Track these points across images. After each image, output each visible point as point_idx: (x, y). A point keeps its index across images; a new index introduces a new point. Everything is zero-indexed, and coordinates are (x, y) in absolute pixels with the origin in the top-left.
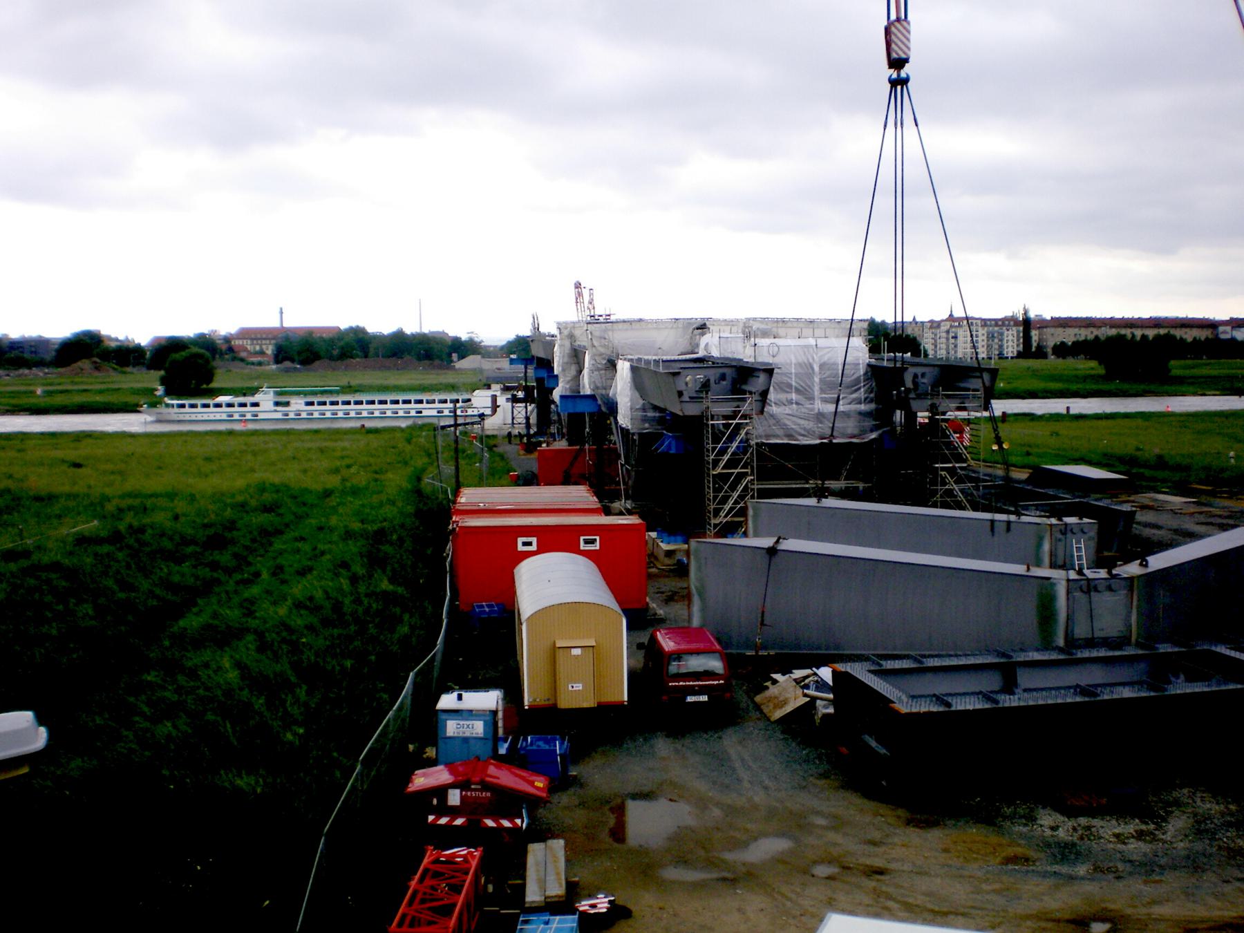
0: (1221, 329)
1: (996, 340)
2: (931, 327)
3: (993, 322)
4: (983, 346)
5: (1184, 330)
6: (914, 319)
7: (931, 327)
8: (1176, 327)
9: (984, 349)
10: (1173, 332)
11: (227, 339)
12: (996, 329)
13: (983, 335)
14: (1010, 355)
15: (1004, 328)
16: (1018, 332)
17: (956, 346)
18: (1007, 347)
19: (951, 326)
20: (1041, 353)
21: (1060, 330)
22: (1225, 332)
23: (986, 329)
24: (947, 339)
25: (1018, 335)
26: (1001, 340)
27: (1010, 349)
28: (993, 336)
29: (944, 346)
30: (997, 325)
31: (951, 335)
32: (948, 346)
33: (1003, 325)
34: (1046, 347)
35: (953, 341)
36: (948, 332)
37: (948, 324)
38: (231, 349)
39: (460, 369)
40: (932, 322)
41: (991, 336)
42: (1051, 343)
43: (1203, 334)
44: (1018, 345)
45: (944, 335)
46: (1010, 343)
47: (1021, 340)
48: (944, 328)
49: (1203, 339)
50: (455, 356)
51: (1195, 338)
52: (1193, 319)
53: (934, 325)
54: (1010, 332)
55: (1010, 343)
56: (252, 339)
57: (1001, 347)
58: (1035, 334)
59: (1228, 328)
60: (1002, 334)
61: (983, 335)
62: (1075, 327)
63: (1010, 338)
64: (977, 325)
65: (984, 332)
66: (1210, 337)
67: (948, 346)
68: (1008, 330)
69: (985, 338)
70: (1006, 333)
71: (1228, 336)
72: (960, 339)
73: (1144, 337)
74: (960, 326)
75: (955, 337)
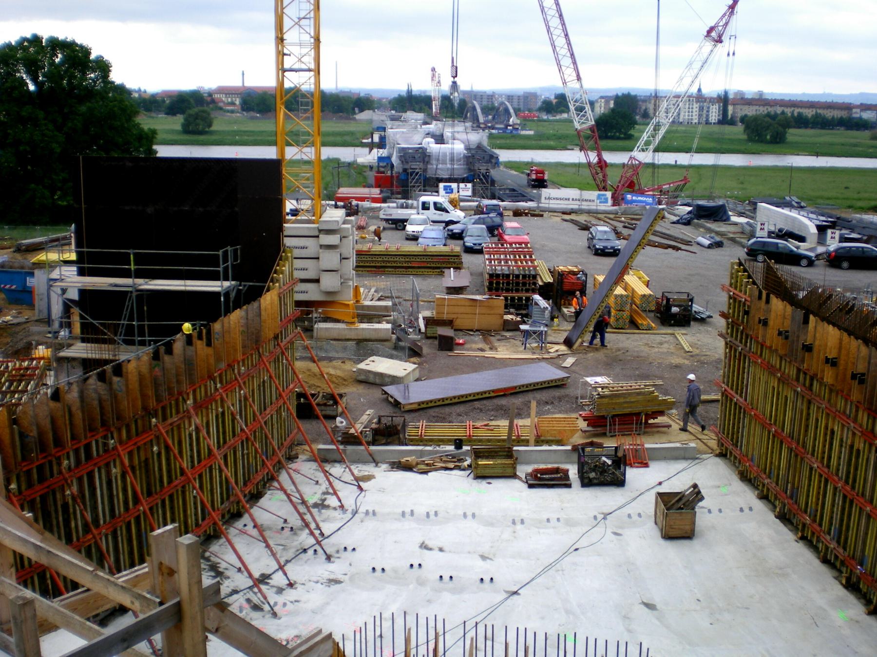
5: (829, 110)
10: (819, 111)
11: (210, 94)
14: (713, 121)
21: (747, 107)
22: (856, 113)
25: (719, 108)
26: (708, 111)
27: (714, 118)
28: (703, 108)
38: (213, 101)
39: (360, 120)
41: (701, 109)
43: (837, 114)
44: (719, 116)
46: (714, 114)
47: (721, 112)
49: (839, 116)
50: (357, 110)
52: (837, 103)
54: (714, 106)
55: (714, 114)
56: (226, 94)
57: (708, 116)
58: (730, 108)
59: (858, 110)
60: (709, 108)
62: (756, 105)
63: (714, 110)
65: (698, 105)
66: (844, 117)
69: (697, 109)
70: (711, 107)
71: (858, 116)
73: (783, 113)
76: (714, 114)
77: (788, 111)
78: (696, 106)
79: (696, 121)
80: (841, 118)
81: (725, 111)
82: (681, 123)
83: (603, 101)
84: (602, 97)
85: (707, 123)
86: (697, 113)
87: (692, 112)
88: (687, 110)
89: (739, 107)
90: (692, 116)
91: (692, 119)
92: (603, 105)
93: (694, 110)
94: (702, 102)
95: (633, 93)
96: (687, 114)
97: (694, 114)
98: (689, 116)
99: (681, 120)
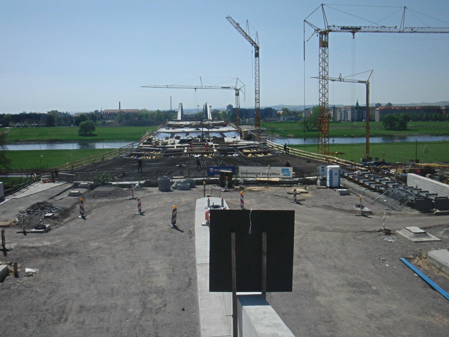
3: (360, 108)
4: (356, 116)
6: (334, 106)
9: (356, 117)
12: (360, 110)
13: (356, 112)
15: (363, 110)
18: (365, 116)
23: (357, 110)
30: (361, 109)
36: (344, 111)
45: (343, 112)
48: (343, 110)
53: (340, 109)
60: (363, 112)
61: (356, 112)
65: (357, 111)
68: (365, 111)
69: (357, 113)
70: (364, 112)
72: (349, 114)
75: (347, 113)
78: (356, 111)
83: (307, 111)
87: (354, 115)
90: (354, 117)
93: (355, 114)
94: (358, 109)
97: (355, 116)
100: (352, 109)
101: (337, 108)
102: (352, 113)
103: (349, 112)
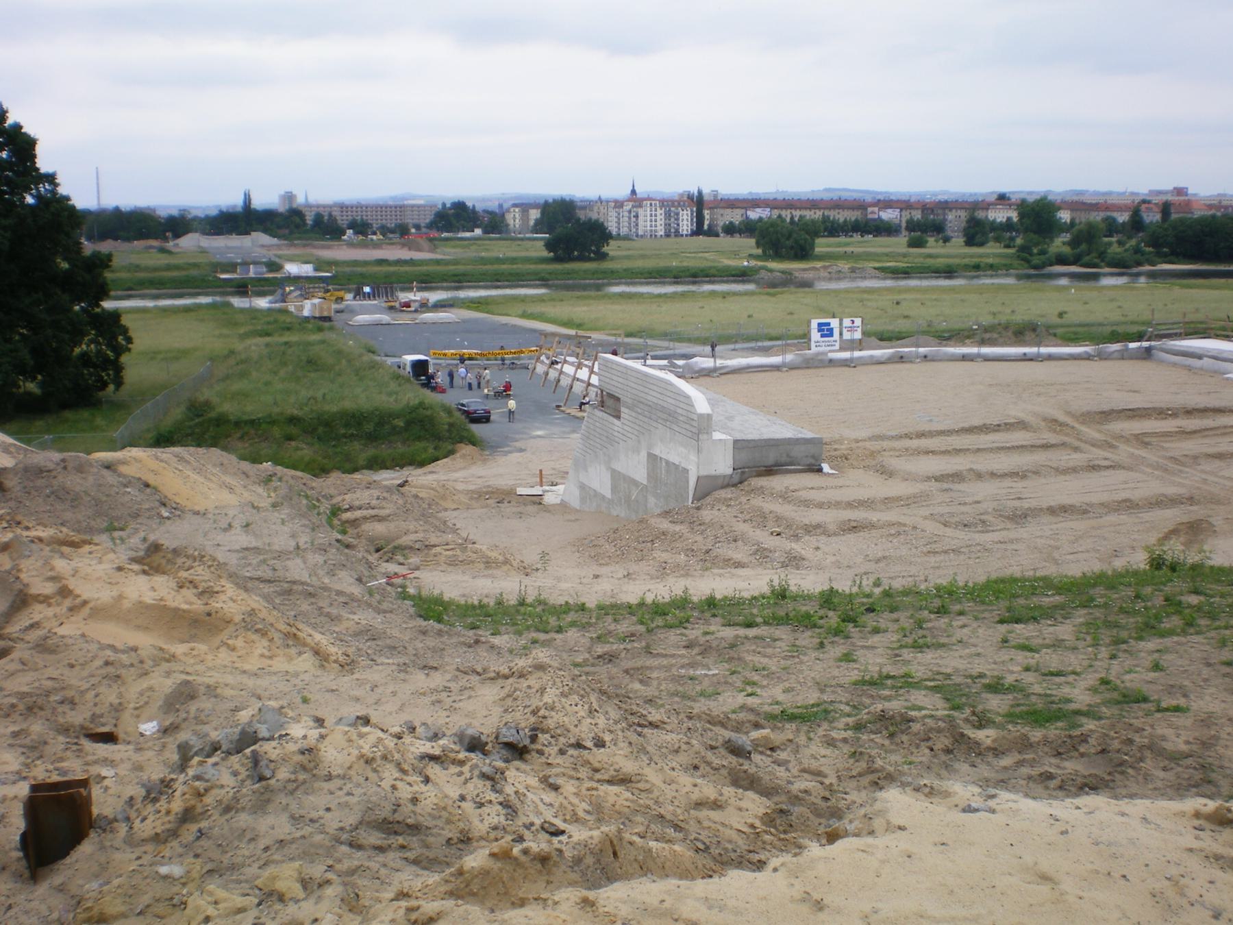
0: (870, 209)
1: (672, 220)
2: (615, 207)
7: (615, 207)
8: (830, 209)
9: (662, 227)
10: (827, 213)
14: (685, 232)
16: (692, 211)
17: (637, 225)
19: (633, 207)
20: (712, 233)
21: (729, 211)
24: (630, 218)
25: (692, 214)
26: (677, 219)
27: (685, 228)
29: (626, 224)
31: (633, 214)
32: (630, 224)
33: (679, 205)
34: (717, 225)
35: (634, 219)
36: (630, 212)
37: (631, 204)
40: (616, 201)
41: (668, 215)
42: (721, 222)
43: (852, 216)
44: (692, 225)
45: (626, 214)
46: (685, 222)
49: (853, 219)
51: (845, 221)
53: (619, 204)
54: (685, 212)
55: (685, 222)
58: (706, 213)
60: (678, 214)
63: (685, 217)
64: (655, 205)
65: (662, 211)
67: (630, 224)
69: (663, 217)
72: (641, 218)
74: (640, 206)
75: (637, 217)
76: (686, 222)
77: (786, 214)
78: (660, 213)
79: (662, 233)
80: (856, 220)
81: (700, 219)
82: (642, 236)
83: (517, 210)
84: (515, 205)
85: (677, 234)
86: (662, 222)
87: (656, 221)
88: (649, 218)
89: (722, 211)
90: (656, 226)
91: (656, 231)
92: (517, 216)
93: (658, 218)
94: (668, 206)
95: (568, 199)
96: (649, 223)
97: (658, 224)
98: (651, 226)
99: (640, 233)
100: (651, 205)
101: (608, 202)
102: (651, 215)
103: (641, 212)
